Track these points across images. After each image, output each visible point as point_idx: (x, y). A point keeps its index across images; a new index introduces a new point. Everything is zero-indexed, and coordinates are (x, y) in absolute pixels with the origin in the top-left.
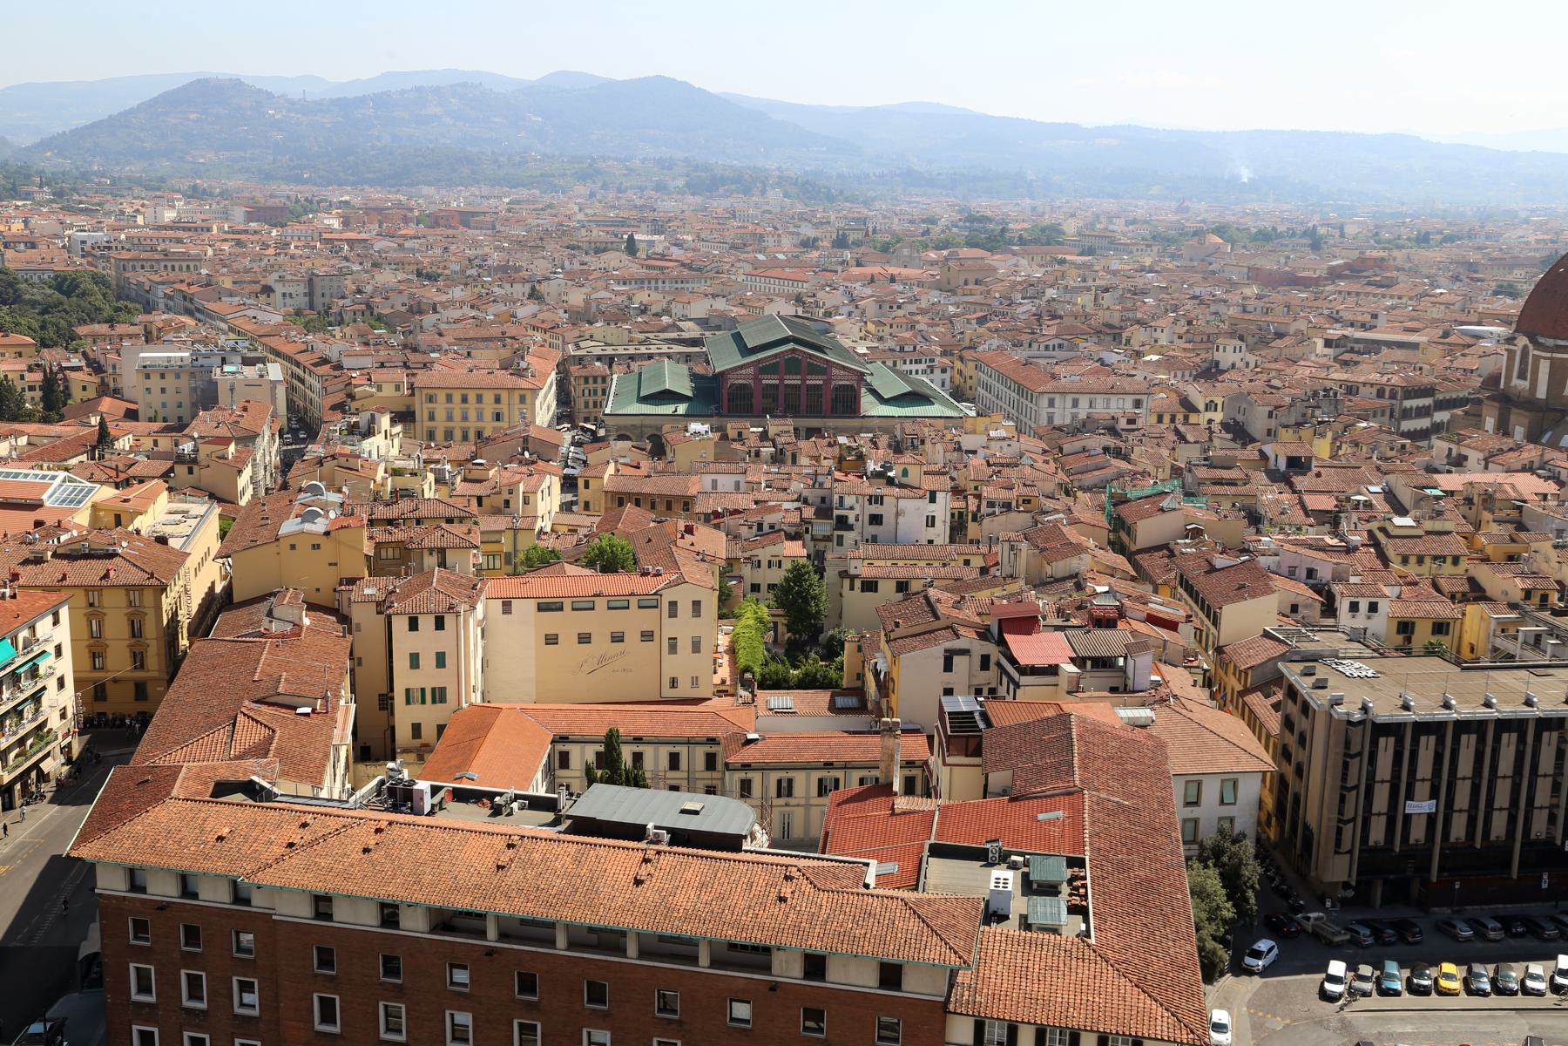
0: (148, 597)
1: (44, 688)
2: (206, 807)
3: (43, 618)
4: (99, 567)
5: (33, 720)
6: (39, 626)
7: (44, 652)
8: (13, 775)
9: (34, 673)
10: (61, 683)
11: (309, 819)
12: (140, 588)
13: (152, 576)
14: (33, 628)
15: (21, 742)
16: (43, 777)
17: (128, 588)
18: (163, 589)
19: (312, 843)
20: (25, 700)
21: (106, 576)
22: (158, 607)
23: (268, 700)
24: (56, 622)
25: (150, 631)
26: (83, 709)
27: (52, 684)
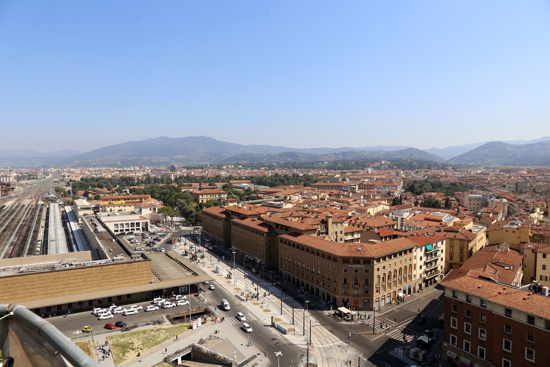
0: (466, 243)
1: (438, 259)
2: (476, 279)
3: (439, 242)
4: (454, 234)
5: (435, 266)
6: (438, 243)
7: (438, 250)
8: (428, 278)
9: (436, 254)
10: (442, 259)
11: (506, 287)
12: (464, 240)
13: (467, 238)
14: (437, 244)
15: (431, 271)
16: (435, 281)
17: (461, 240)
18: (470, 241)
19: (506, 294)
20: (433, 261)
21: (455, 236)
22: (468, 246)
23: (496, 264)
24: (442, 244)
25: (465, 252)
26: (446, 267)
27: (440, 259)
